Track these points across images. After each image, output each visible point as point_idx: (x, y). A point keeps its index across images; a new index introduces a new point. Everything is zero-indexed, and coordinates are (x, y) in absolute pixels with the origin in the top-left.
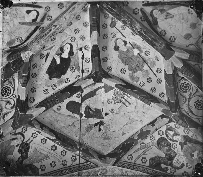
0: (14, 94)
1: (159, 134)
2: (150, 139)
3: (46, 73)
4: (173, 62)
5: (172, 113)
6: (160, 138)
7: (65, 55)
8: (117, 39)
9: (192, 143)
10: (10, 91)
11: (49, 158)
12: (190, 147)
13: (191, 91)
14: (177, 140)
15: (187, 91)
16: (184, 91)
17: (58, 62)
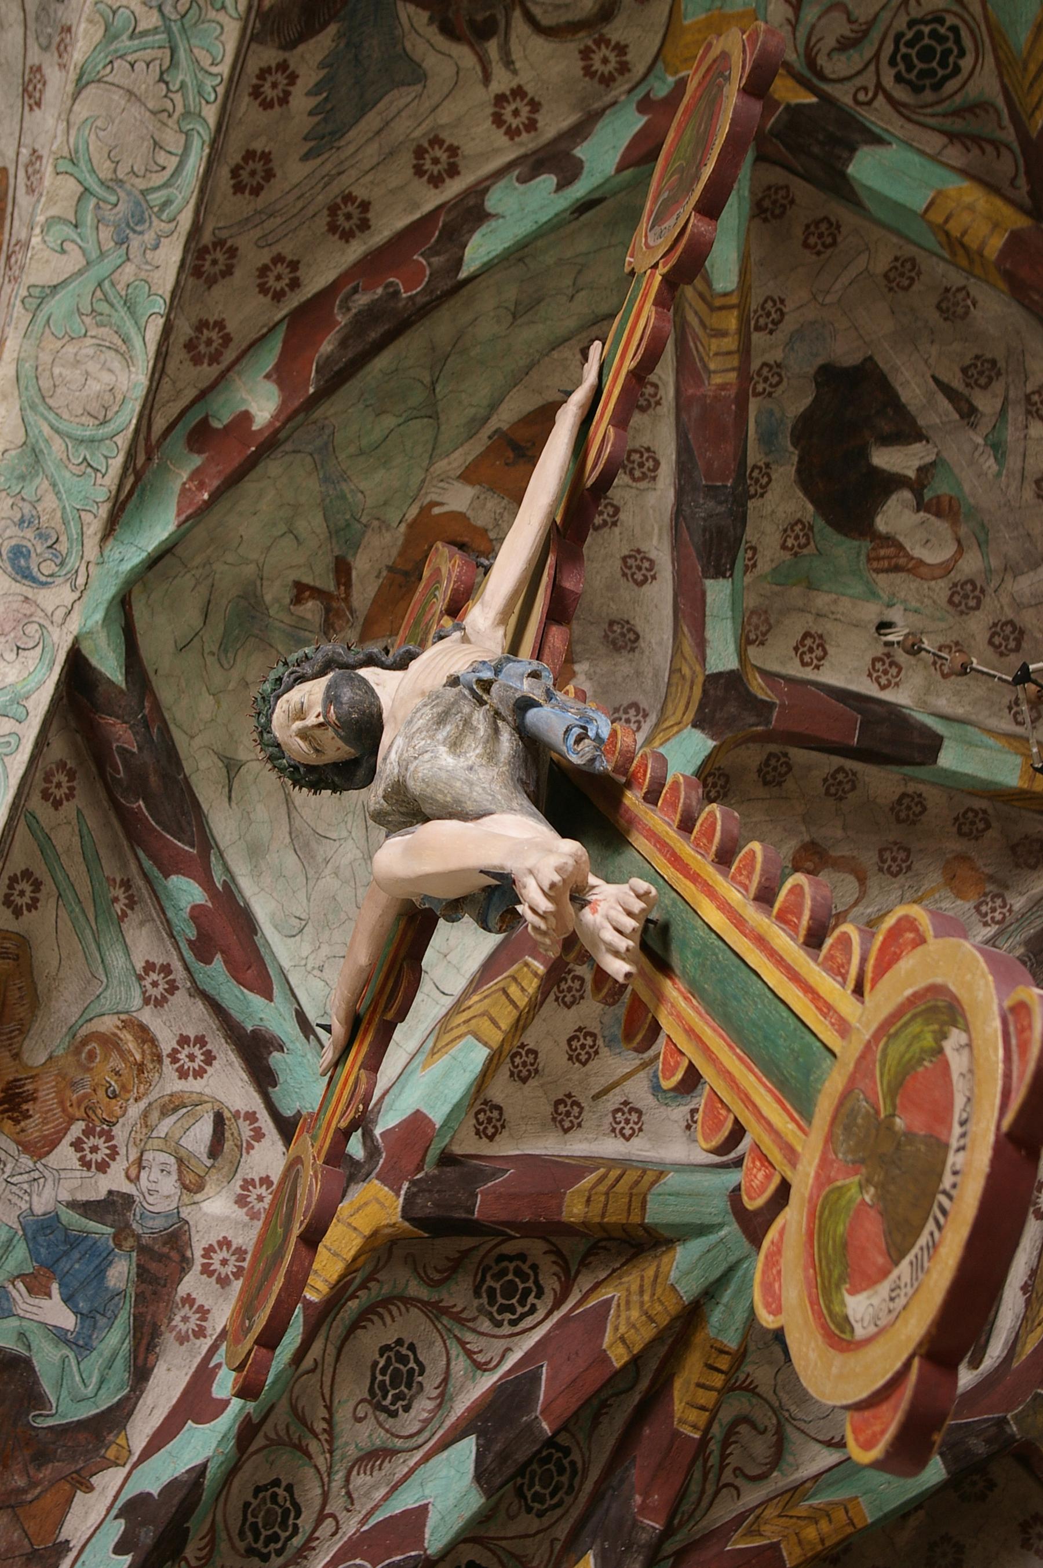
0: (881, 97)
1: (184, 1041)
2: (149, 967)
3: (870, 358)
4: (713, 1238)
5: (406, 1185)
6: (153, 1041)
7: (896, 516)
8: (862, 880)
9: (140, 1297)
10: (909, 83)
11: (306, 157)
12: (100, 1273)
13: (486, 1325)
14: (144, 1175)
15: (485, 1300)
16: (483, 1280)
17: (887, 459)
